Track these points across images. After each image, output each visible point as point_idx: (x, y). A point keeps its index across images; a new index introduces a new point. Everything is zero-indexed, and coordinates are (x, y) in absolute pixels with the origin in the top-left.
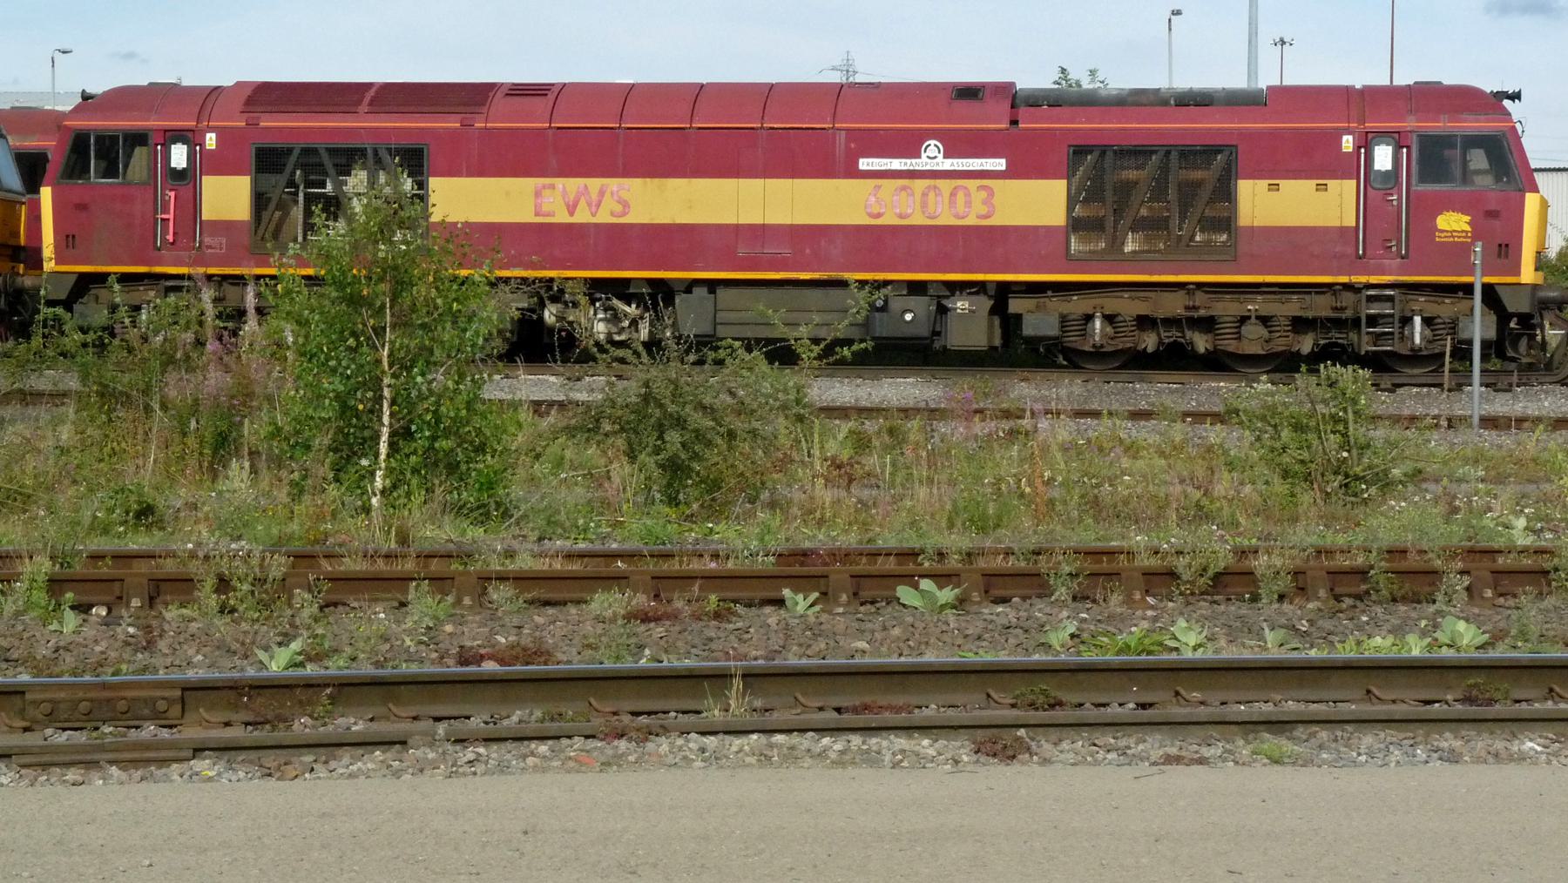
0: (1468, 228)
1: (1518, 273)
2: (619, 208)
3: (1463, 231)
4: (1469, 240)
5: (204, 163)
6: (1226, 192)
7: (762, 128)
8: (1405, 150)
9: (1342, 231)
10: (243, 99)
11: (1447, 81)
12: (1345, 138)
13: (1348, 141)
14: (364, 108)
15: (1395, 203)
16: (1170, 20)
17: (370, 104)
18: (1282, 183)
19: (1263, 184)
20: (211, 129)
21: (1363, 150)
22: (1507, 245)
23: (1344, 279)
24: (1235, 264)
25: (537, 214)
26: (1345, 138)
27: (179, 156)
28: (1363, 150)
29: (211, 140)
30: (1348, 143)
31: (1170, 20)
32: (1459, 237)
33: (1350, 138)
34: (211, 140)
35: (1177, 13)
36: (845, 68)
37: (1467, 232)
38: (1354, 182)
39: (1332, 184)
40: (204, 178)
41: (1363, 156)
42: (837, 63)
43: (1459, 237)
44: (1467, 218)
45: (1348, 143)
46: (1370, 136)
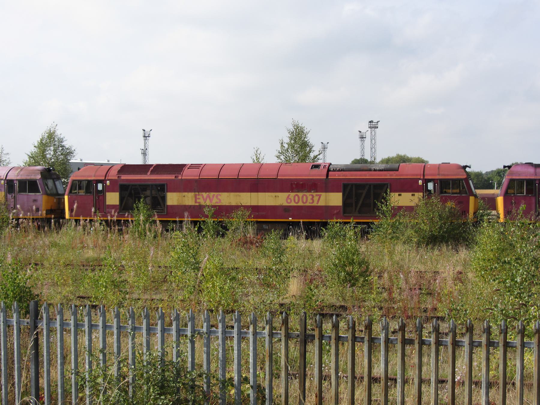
2: (218, 201)
5: (106, 189)
10: (117, 171)
12: (420, 181)
14: (149, 173)
17: (151, 172)
18: (402, 193)
19: (397, 194)
20: (109, 180)
25: (196, 202)
26: (420, 181)
27: (100, 187)
29: (108, 182)
30: (420, 182)
33: (421, 181)
34: (108, 182)
40: (107, 193)
45: (420, 182)
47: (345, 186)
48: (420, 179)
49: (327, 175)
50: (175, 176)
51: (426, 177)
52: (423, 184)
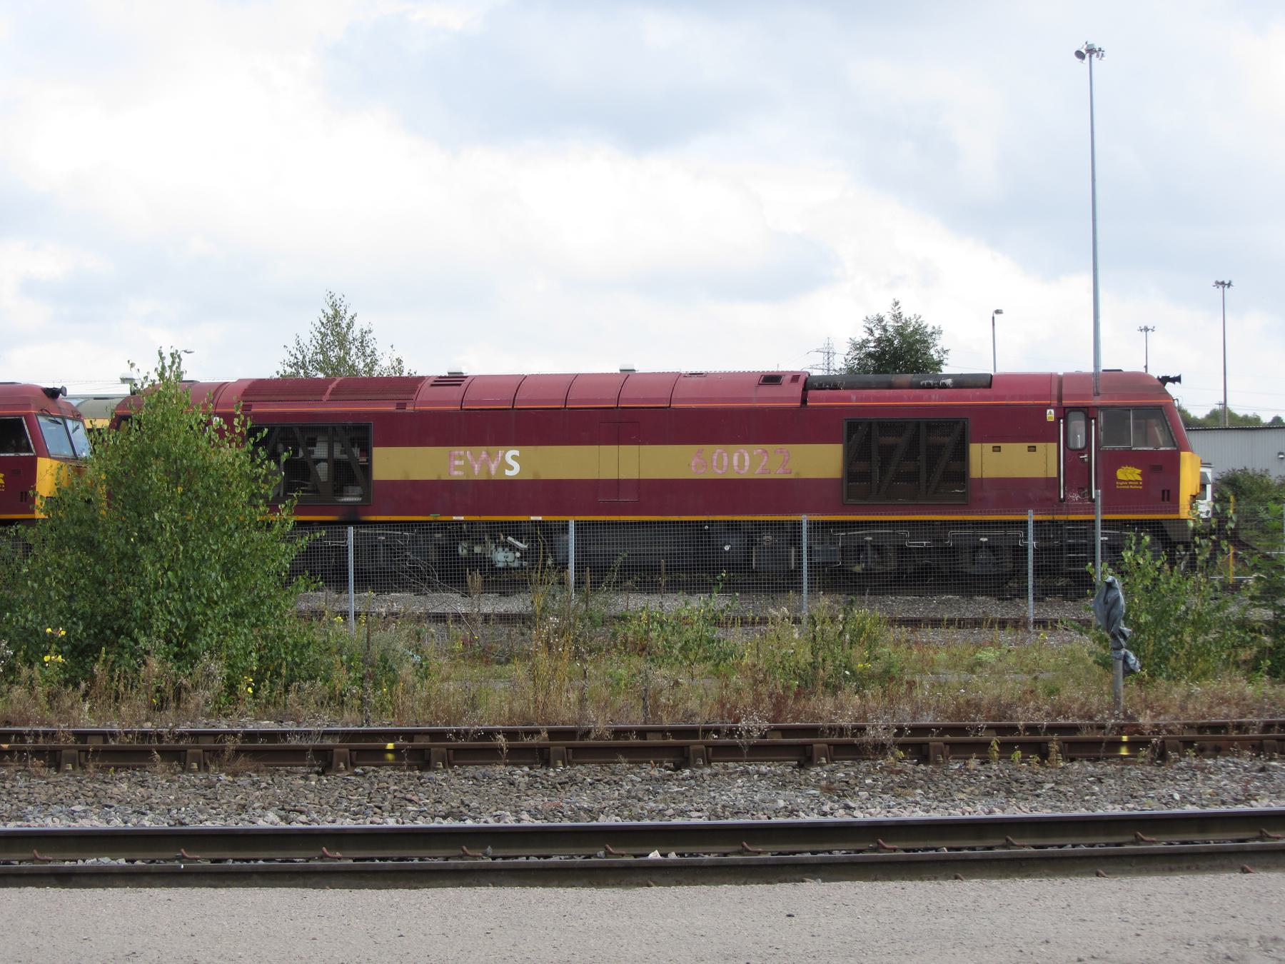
0: (1139, 478)
1: (1177, 511)
3: (1136, 481)
4: (1141, 487)
6: (962, 455)
7: (617, 407)
8: (1093, 421)
9: (1048, 480)
10: (241, 393)
11: (1126, 369)
13: (1050, 413)
14: (327, 397)
15: (1086, 460)
16: (993, 318)
18: (1003, 445)
21: (1062, 421)
22: (1168, 491)
23: (1050, 517)
24: (965, 506)
26: (1048, 411)
28: (1062, 421)
30: (1050, 414)
31: (993, 318)
32: (1133, 485)
33: (1052, 411)
35: (998, 312)
36: (826, 350)
37: (1139, 481)
38: (1055, 445)
39: (1039, 446)
41: (1062, 425)
42: (820, 346)
43: (1133, 485)
44: (1139, 471)
45: (1050, 414)
46: (1067, 410)
47: (853, 427)
48: (1049, 406)
49: (804, 401)
50: (398, 404)
51: (1065, 402)
52: (1058, 419)
